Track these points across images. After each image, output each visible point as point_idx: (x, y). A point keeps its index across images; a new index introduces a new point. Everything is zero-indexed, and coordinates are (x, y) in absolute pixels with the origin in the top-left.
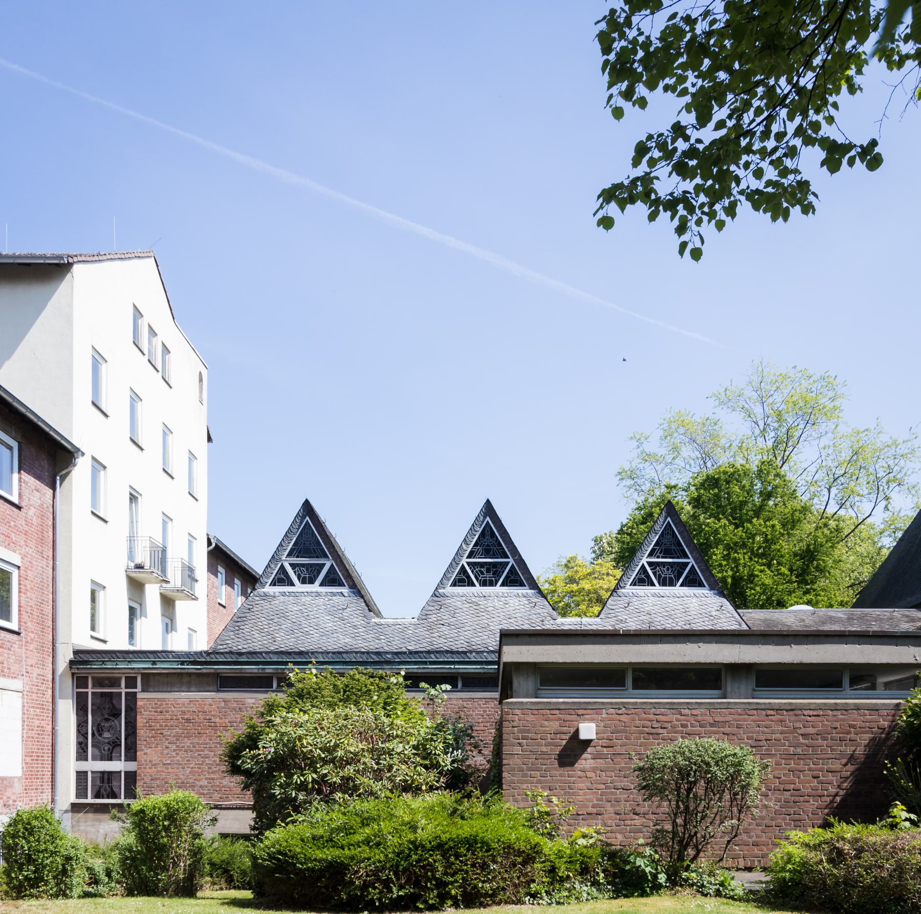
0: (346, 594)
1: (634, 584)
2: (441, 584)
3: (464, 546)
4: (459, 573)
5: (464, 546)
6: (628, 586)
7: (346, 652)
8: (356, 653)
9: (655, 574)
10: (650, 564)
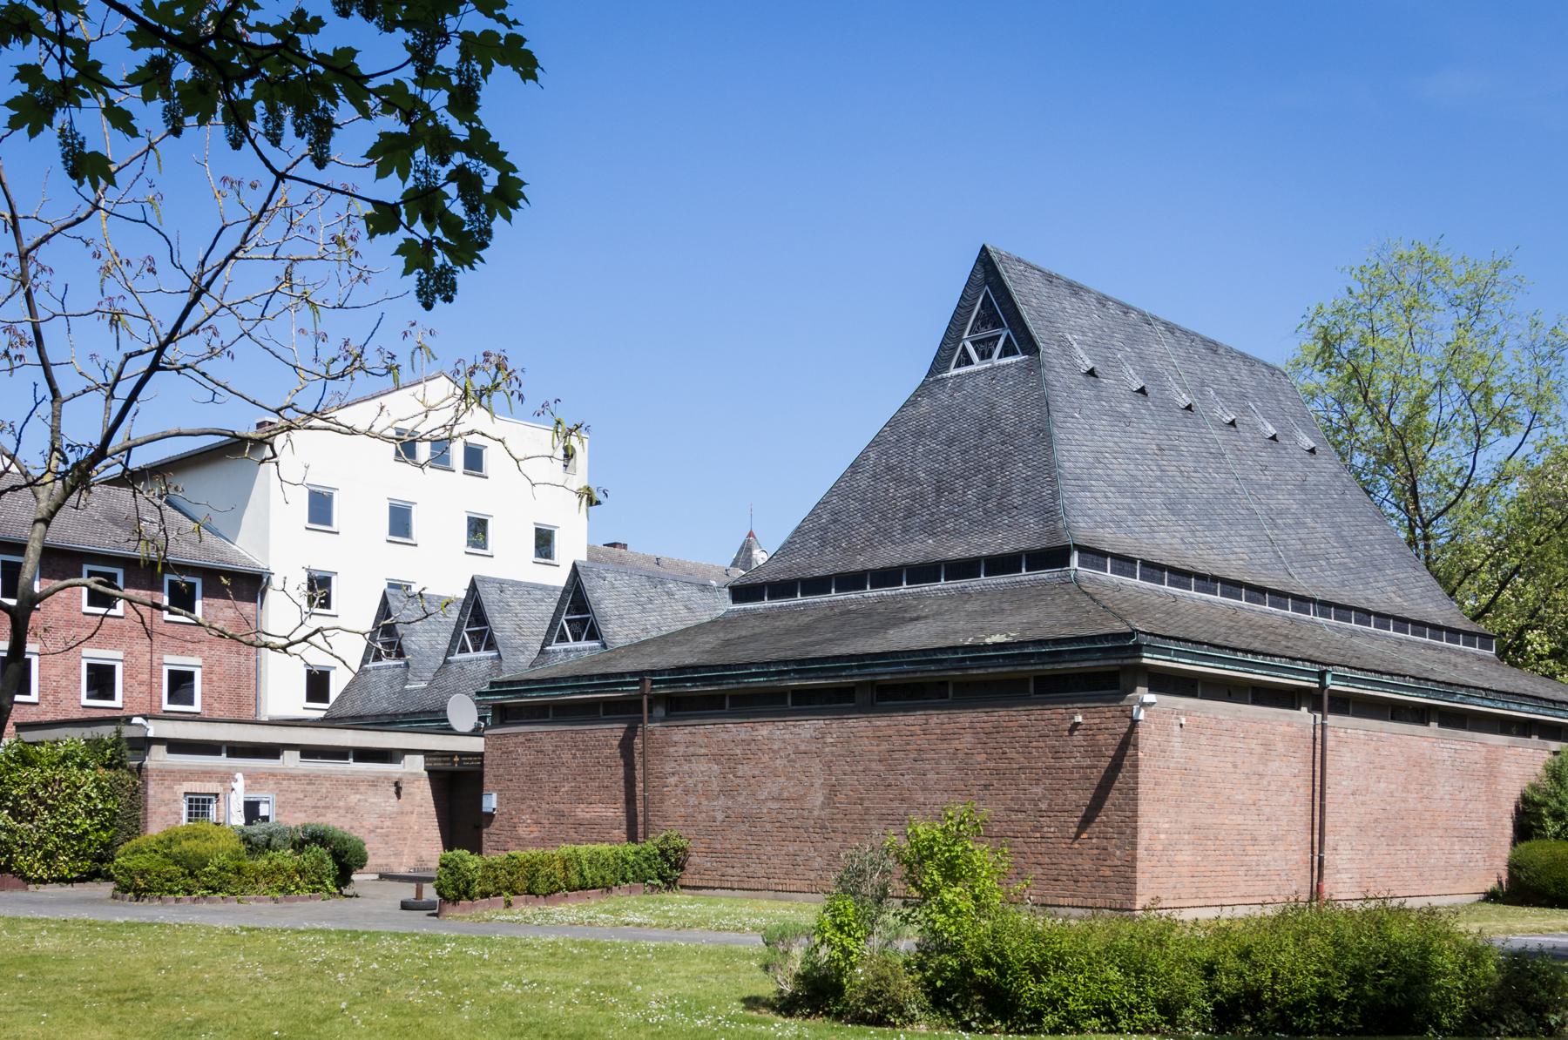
2: (449, 652)
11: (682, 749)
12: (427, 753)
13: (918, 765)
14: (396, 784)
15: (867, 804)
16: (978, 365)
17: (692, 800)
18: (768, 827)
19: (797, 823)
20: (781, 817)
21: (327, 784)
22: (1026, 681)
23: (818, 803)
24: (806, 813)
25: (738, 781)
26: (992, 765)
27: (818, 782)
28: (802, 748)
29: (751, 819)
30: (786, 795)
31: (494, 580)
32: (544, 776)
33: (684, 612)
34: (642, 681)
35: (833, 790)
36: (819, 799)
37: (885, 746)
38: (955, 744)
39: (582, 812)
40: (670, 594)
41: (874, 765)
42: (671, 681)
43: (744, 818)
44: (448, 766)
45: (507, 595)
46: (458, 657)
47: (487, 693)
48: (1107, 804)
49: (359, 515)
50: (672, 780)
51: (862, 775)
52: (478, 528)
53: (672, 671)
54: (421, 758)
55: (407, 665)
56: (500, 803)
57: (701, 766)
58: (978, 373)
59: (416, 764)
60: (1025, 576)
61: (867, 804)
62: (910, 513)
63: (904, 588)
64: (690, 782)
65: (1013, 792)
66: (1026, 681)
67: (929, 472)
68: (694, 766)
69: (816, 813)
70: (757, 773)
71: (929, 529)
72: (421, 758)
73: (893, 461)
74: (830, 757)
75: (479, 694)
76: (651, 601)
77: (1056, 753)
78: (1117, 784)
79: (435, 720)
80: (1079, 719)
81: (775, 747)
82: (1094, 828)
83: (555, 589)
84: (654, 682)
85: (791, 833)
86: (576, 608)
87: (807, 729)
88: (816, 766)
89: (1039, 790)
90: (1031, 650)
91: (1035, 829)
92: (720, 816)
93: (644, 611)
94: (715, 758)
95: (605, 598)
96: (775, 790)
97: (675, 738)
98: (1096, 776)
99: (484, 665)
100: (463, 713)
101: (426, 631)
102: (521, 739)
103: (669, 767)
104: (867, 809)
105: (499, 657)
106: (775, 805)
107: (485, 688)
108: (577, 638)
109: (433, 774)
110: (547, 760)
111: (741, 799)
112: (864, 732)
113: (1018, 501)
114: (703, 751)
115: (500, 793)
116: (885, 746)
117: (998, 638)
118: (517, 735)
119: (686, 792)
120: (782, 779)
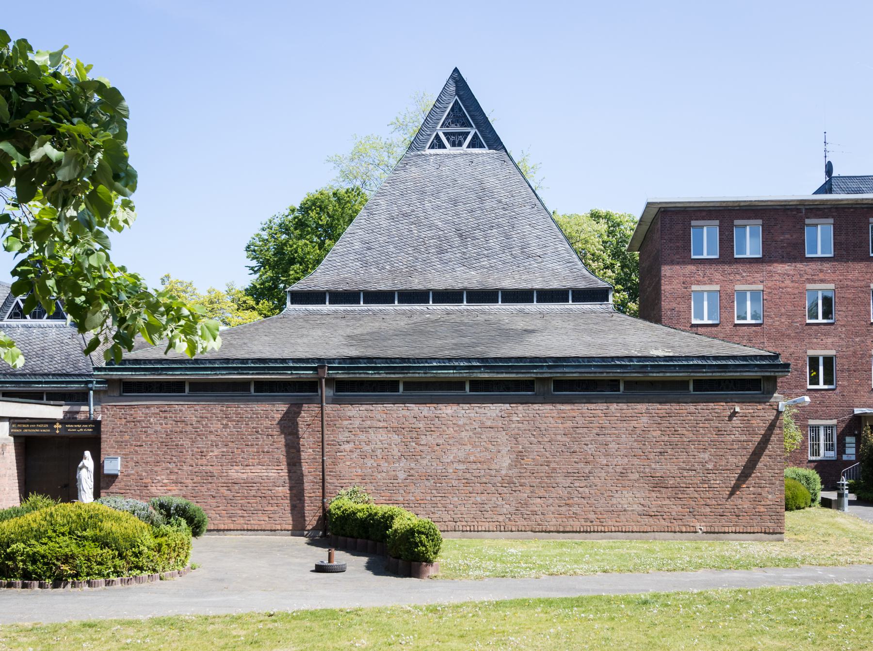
1: (10, 317)
6: (5, 319)
11: (357, 423)
12: (14, 421)
13: (601, 438)
15: (553, 465)
16: (449, 150)
17: (369, 462)
18: (455, 483)
19: (484, 480)
20: (468, 475)
22: (687, 382)
23: (506, 465)
24: (493, 473)
25: (419, 448)
26: (666, 438)
27: (504, 450)
28: (489, 423)
29: (439, 478)
30: (472, 458)
32: (187, 443)
34: (323, 367)
35: (520, 456)
36: (506, 462)
37: (569, 424)
38: (634, 424)
39: (236, 473)
41: (559, 437)
43: (428, 477)
48: (760, 465)
50: (348, 447)
51: (548, 446)
56: (125, 466)
57: (382, 435)
58: (447, 156)
60: (571, 306)
61: (553, 465)
62: (441, 251)
63: (464, 306)
65: (684, 456)
66: (687, 382)
67: (447, 222)
68: (372, 435)
69: (504, 472)
70: (441, 441)
71: (466, 262)
73: (406, 209)
74: (516, 431)
77: (719, 432)
78: (767, 452)
80: (737, 409)
81: (460, 423)
82: (751, 481)
84: (330, 368)
85: (479, 488)
87: (493, 411)
88: (503, 437)
89: (706, 456)
90: (695, 362)
91: (704, 482)
92: (402, 475)
94: (396, 430)
96: (461, 455)
97: (350, 414)
98: (751, 447)
103: (342, 437)
104: (554, 469)
106: (462, 467)
109: (16, 437)
110: (189, 428)
111: (424, 462)
112: (549, 416)
113: (539, 252)
114: (381, 424)
115: (125, 457)
116: (569, 424)
117: (660, 353)
118: (148, 407)
119: (363, 456)
120: (469, 447)
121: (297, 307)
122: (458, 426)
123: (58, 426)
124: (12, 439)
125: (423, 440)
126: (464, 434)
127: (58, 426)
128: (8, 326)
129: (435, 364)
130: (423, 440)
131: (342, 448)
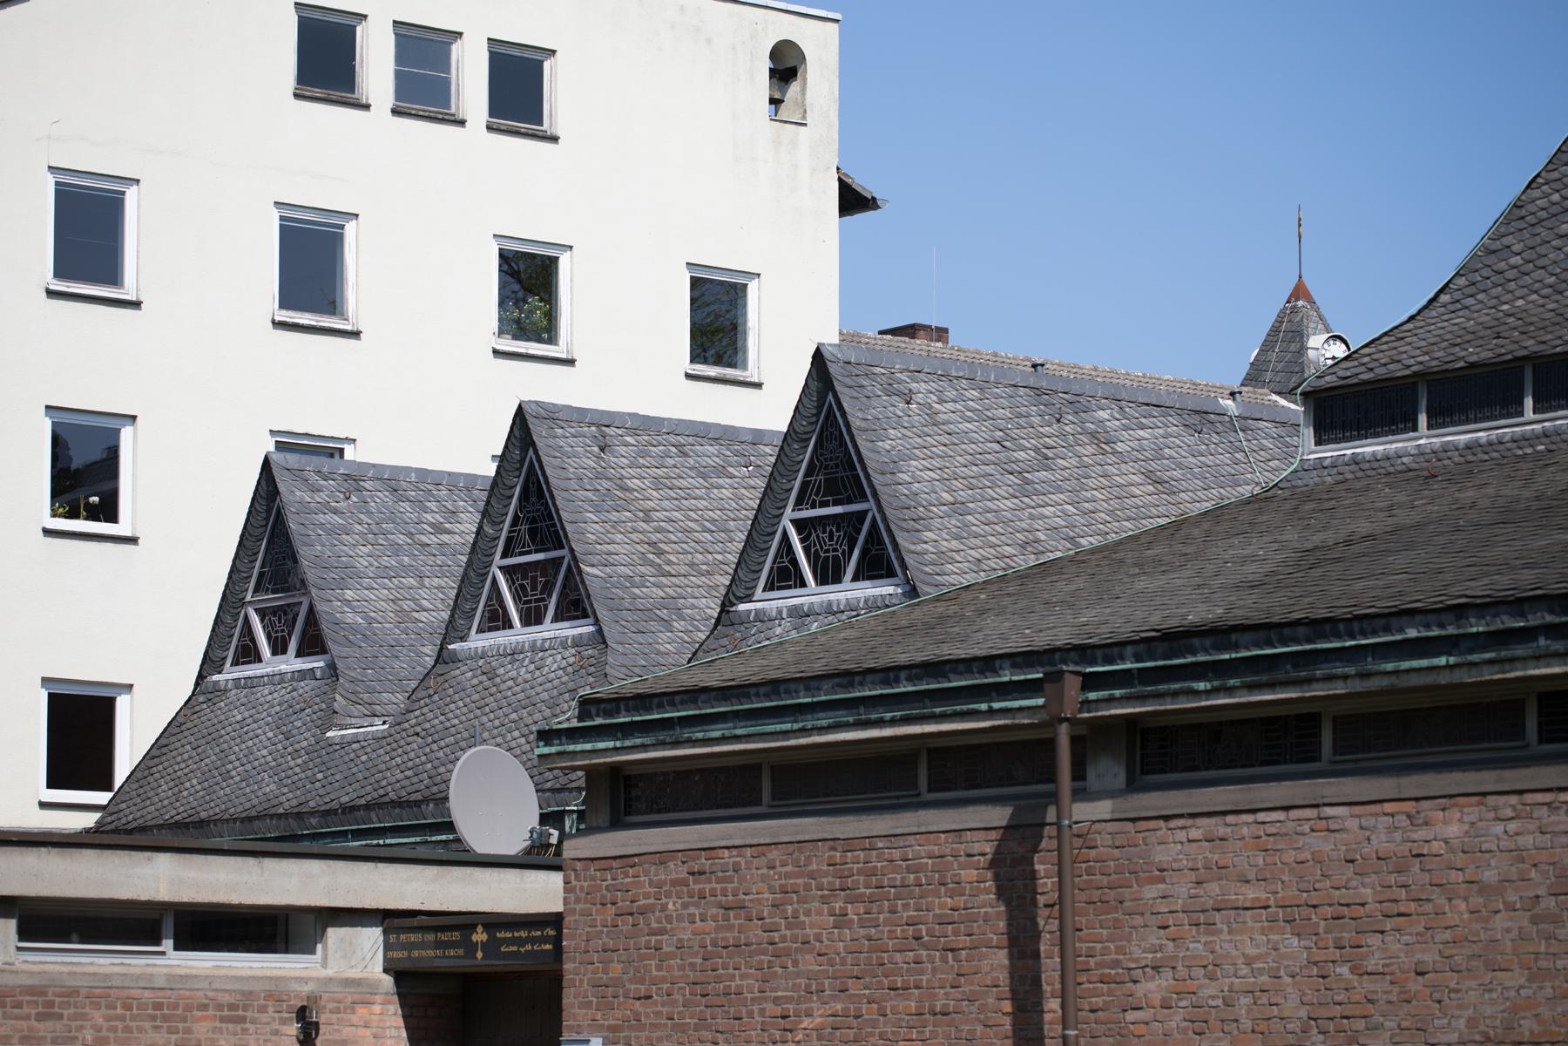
0: (318, 674)
1: (770, 587)
2: (453, 630)
3: (488, 530)
4: (489, 598)
5: (488, 530)
6: (759, 593)
7: (257, 818)
8: (272, 816)
9: (807, 550)
10: (800, 525)
11: (1182, 890)
14: (302, 1013)
21: (98, 1017)
25: (1369, 985)
31: (581, 416)
32: (748, 983)
33: (1143, 492)
34: (1056, 677)
40: (1102, 439)
42: (1145, 676)
44: (453, 959)
45: (621, 457)
46: (478, 642)
47: (573, 734)
49: (200, 252)
50: (1153, 988)
52: (529, 282)
53: (1147, 644)
54: (371, 939)
55: (332, 670)
57: (1245, 943)
59: (359, 955)
64: (1209, 991)
68: (1223, 943)
70: (1429, 957)
72: (371, 939)
75: (546, 736)
76: (1045, 462)
79: (416, 825)
81: (1490, 876)
83: (758, 437)
84: (1090, 682)
86: (827, 483)
93: (1025, 488)
94: (1293, 916)
95: (909, 456)
97: (1161, 856)
99: (552, 662)
100: (496, 801)
101: (384, 572)
102: (676, 870)
103: (1141, 947)
105: (600, 638)
107: (568, 718)
108: (828, 573)
109: (405, 978)
110: (756, 933)
114: (1251, 893)
120: (1516, 978)
121: (1330, 452)
122: (1484, 889)
123: (480, 936)
124: (388, 981)
125: (1376, 953)
126: (1499, 922)
127: (480, 936)
128: (760, 617)
129: (1412, 633)
130: (1376, 953)
131: (1139, 990)
